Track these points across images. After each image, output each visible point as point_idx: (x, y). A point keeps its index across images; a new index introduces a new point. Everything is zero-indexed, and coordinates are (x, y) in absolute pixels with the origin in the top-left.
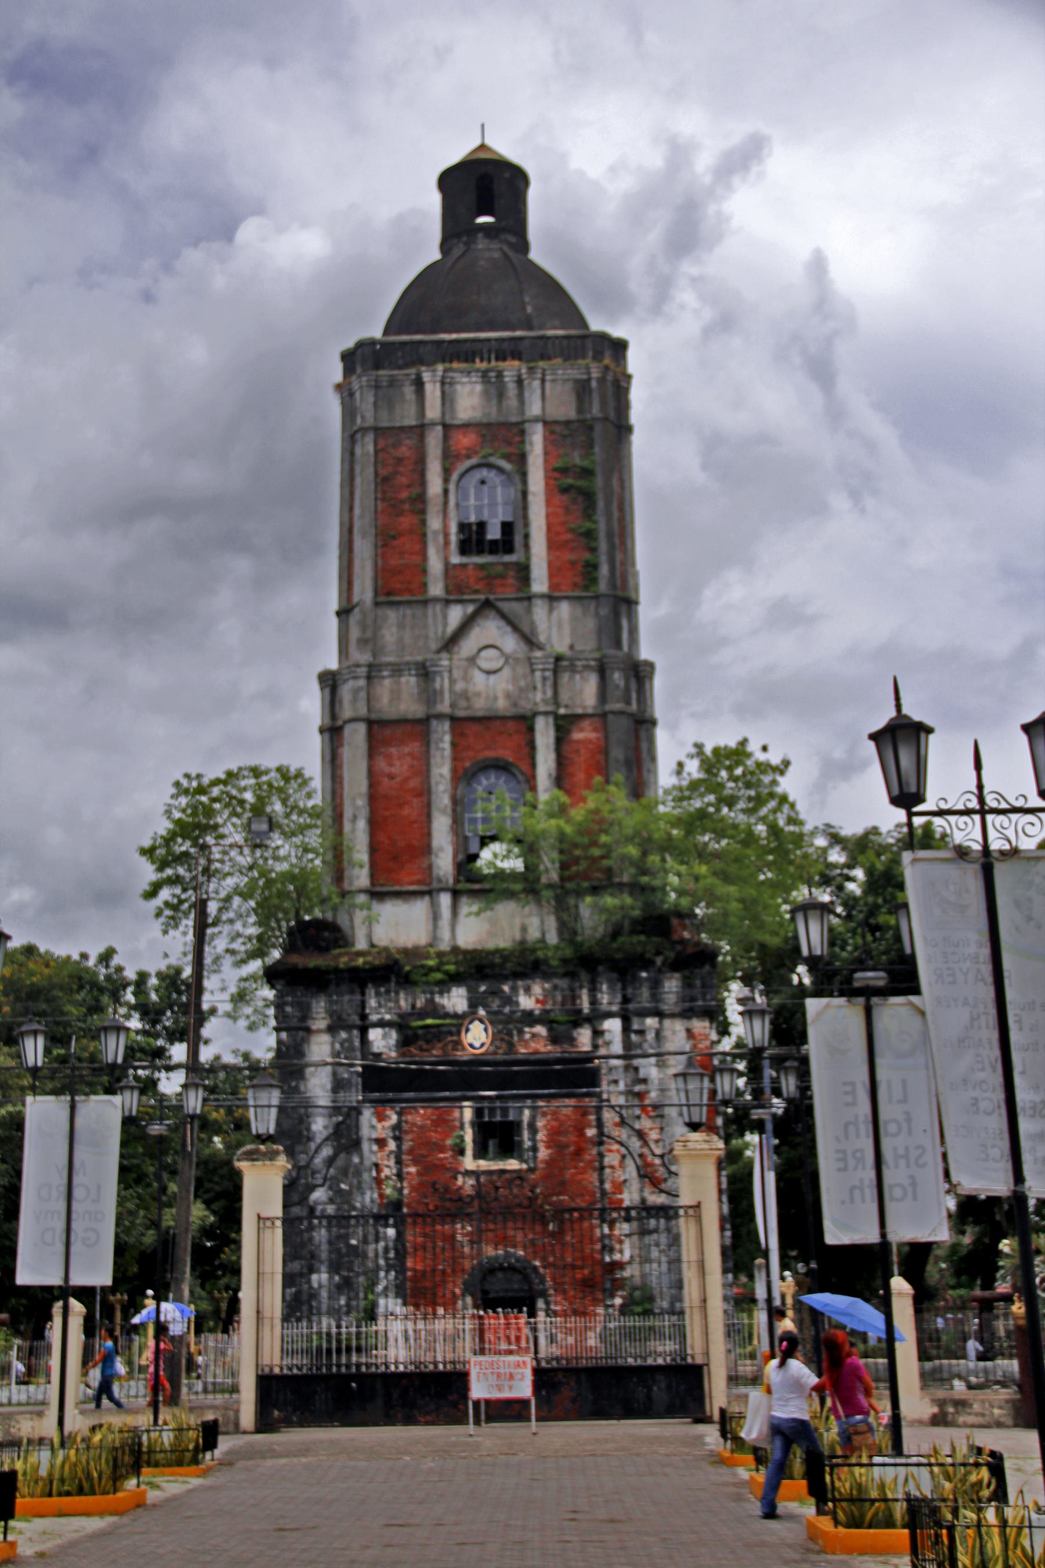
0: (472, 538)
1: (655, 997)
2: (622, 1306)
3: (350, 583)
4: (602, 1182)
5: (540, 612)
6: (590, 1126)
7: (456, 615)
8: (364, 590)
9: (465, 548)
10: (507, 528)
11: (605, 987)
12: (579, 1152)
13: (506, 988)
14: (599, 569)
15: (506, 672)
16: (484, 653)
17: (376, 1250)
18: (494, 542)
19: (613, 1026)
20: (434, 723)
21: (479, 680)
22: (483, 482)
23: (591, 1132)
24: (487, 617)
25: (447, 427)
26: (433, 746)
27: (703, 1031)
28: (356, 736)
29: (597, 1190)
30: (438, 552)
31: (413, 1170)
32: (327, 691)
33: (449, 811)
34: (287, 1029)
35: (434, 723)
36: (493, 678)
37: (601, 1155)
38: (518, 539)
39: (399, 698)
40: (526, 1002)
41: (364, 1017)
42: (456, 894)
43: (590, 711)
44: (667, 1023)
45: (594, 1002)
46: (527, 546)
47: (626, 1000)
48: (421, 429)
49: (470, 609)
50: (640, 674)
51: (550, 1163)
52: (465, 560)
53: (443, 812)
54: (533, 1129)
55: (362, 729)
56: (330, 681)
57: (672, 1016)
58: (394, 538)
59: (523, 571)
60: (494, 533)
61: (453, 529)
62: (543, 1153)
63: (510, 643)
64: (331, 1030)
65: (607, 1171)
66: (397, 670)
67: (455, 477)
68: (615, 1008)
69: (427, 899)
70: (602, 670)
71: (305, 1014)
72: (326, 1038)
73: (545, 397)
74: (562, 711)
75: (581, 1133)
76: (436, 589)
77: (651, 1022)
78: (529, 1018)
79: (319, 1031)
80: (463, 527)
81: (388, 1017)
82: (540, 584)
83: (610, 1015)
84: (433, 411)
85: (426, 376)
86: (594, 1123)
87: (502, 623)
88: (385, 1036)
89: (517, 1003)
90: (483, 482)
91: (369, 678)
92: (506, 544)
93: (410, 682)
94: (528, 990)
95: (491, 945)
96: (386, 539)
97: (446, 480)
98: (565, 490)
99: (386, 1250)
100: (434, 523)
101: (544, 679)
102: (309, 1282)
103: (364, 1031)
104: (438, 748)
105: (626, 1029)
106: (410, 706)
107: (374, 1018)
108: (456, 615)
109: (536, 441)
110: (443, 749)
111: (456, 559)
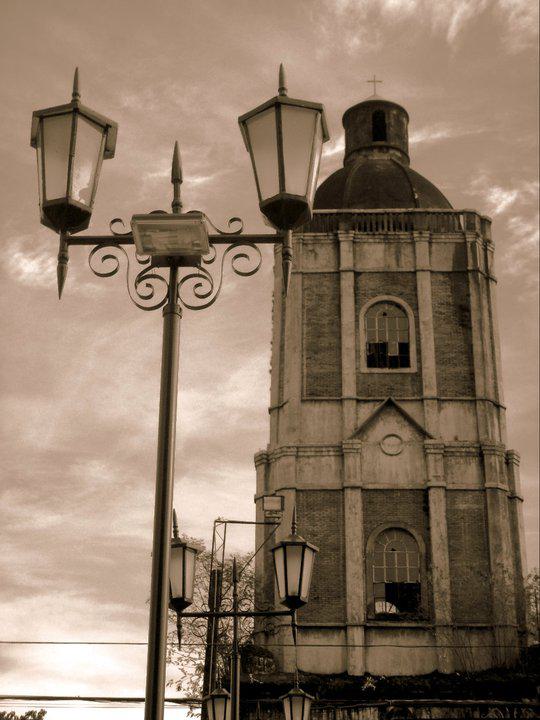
3: (281, 387)
7: (366, 411)
8: (293, 389)
9: (371, 363)
15: (406, 455)
16: (387, 441)
20: (348, 492)
21: (384, 459)
22: (385, 314)
24: (389, 413)
25: (357, 274)
32: (262, 467)
33: (360, 562)
39: (321, 473)
42: (367, 629)
46: (419, 361)
48: (337, 274)
49: (378, 406)
56: (264, 461)
58: (316, 353)
59: (418, 377)
60: (393, 351)
63: (407, 433)
66: (319, 450)
67: (363, 310)
73: (430, 256)
76: (349, 390)
82: (430, 390)
84: (347, 261)
85: (342, 237)
87: (401, 419)
90: (385, 314)
92: (403, 360)
93: (330, 461)
95: (395, 672)
96: (312, 351)
97: (357, 310)
106: (329, 480)
109: (425, 284)
111: (365, 369)
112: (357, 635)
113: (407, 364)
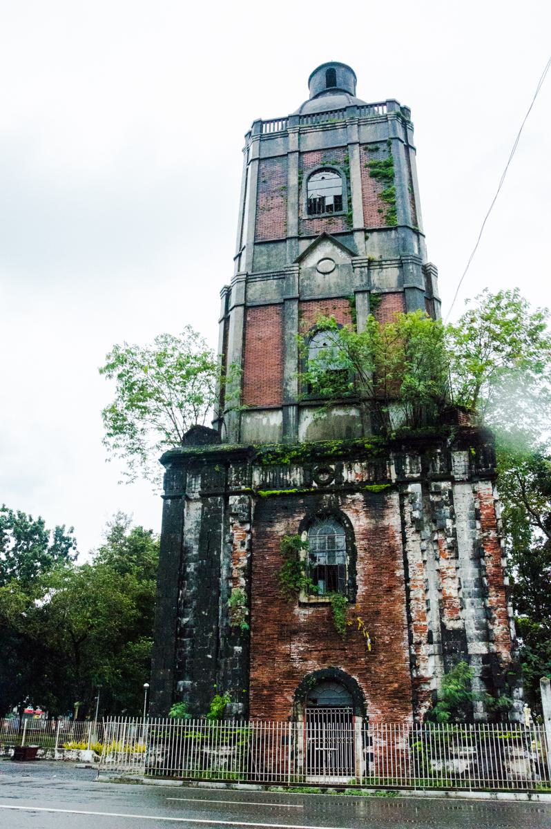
0: (315, 207)
1: (448, 465)
2: (426, 714)
4: (409, 610)
5: (359, 237)
6: (398, 569)
7: (305, 244)
10: (338, 199)
11: (408, 460)
12: (390, 590)
13: (333, 467)
14: (399, 222)
17: (226, 663)
18: (330, 207)
19: (415, 488)
23: (400, 573)
26: (287, 316)
27: (487, 492)
28: (236, 316)
29: (405, 618)
30: (294, 213)
31: (259, 602)
34: (172, 498)
35: (288, 303)
36: (327, 276)
37: (408, 590)
38: (345, 204)
40: (348, 476)
41: (227, 486)
43: (393, 290)
44: (458, 488)
45: (400, 472)
47: (425, 471)
50: (428, 272)
51: (367, 597)
52: (311, 217)
53: (293, 357)
54: (353, 572)
55: (241, 309)
57: (462, 482)
60: (329, 201)
61: (304, 201)
62: (362, 589)
64: (203, 497)
65: (412, 602)
66: (266, 277)
68: (415, 475)
69: (280, 413)
70: (401, 265)
71: (184, 487)
72: (200, 505)
74: (374, 291)
75: (393, 575)
77: (444, 485)
78: (351, 488)
79: (196, 500)
80: (309, 201)
81: (243, 487)
82: (358, 223)
83: (414, 481)
86: (402, 566)
88: (241, 501)
89: (342, 477)
91: (247, 282)
94: (350, 468)
98: (373, 175)
99: (233, 664)
100: (292, 199)
101: (361, 272)
102: (175, 685)
103: (227, 500)
104: (290, 318)
105: (426, 490)
107: (234, 488)
108: (305, 244)
110: (293, 318)
111: (305, 216)
112: (292, 411)
113: (341, 209)
